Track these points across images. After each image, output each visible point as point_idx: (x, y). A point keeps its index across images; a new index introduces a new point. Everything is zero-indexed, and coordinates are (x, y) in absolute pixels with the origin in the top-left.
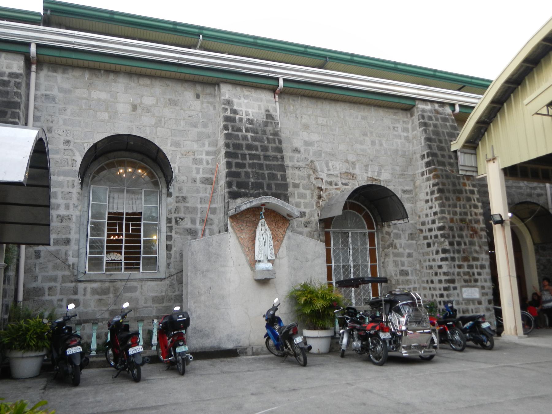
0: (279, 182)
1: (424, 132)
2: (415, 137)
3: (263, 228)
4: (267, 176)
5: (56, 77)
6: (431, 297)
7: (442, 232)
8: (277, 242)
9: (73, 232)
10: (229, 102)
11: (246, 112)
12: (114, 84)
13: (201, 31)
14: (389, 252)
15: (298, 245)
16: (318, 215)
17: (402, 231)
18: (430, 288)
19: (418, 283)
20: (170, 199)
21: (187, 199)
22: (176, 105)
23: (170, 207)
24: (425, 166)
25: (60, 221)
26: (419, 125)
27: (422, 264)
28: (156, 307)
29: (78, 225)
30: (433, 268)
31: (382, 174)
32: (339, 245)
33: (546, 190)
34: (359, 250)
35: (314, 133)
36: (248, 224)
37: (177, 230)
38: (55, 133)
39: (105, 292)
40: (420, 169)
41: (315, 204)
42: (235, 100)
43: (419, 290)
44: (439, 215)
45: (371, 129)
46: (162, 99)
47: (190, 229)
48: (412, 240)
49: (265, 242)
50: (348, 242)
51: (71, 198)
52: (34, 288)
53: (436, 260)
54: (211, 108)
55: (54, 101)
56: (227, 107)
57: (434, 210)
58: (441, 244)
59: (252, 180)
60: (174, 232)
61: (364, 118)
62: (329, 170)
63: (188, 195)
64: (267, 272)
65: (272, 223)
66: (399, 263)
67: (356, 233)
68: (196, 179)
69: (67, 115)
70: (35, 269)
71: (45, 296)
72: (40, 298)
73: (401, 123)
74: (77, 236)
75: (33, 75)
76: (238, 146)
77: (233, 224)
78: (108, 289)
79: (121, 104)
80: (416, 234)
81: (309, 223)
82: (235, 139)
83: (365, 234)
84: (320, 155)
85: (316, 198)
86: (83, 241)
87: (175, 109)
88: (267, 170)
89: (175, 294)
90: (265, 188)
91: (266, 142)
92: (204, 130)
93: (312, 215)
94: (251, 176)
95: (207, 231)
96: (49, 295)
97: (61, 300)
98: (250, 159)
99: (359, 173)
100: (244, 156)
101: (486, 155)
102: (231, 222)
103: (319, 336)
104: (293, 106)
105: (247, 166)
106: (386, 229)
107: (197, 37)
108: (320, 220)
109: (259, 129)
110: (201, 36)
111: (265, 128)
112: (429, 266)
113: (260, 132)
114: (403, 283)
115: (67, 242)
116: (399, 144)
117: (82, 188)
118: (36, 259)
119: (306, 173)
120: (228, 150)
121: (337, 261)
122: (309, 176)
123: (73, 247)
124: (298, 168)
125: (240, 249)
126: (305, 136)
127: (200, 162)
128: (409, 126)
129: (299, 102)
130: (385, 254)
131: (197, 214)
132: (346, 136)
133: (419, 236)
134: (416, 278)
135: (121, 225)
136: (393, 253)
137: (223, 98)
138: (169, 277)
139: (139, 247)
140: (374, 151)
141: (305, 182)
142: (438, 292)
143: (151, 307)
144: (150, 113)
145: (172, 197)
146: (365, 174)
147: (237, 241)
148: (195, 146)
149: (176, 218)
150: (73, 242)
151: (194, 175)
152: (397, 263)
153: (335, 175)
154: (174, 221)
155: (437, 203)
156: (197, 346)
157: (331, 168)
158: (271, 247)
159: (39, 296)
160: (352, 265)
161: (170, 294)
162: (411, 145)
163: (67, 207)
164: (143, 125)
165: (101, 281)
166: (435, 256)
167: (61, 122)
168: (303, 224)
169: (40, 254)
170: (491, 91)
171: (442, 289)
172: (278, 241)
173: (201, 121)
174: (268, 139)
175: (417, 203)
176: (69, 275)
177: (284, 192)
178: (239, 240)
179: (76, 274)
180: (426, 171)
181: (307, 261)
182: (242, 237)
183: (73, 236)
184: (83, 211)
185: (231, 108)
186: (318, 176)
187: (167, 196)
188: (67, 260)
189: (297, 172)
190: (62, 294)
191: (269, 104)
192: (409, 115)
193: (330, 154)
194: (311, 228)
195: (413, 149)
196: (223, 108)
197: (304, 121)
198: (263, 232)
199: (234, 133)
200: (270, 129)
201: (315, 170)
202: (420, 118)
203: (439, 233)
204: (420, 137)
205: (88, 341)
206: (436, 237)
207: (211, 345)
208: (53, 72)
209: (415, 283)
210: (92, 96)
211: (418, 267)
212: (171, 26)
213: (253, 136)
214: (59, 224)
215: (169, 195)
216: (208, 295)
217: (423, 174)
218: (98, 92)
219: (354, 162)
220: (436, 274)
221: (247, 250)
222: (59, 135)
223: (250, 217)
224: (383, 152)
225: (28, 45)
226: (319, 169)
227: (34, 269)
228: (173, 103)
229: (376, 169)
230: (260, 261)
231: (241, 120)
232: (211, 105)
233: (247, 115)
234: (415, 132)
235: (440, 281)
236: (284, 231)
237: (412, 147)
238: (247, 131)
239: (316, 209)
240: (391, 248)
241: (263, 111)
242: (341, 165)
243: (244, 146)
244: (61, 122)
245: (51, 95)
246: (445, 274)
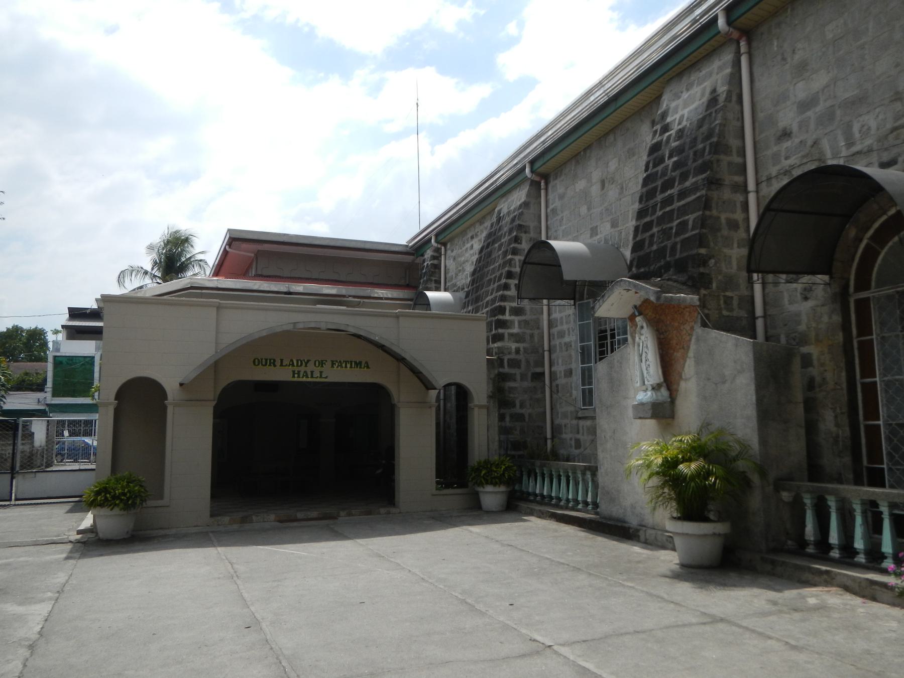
153: (865, 150)
181: (724, 382)
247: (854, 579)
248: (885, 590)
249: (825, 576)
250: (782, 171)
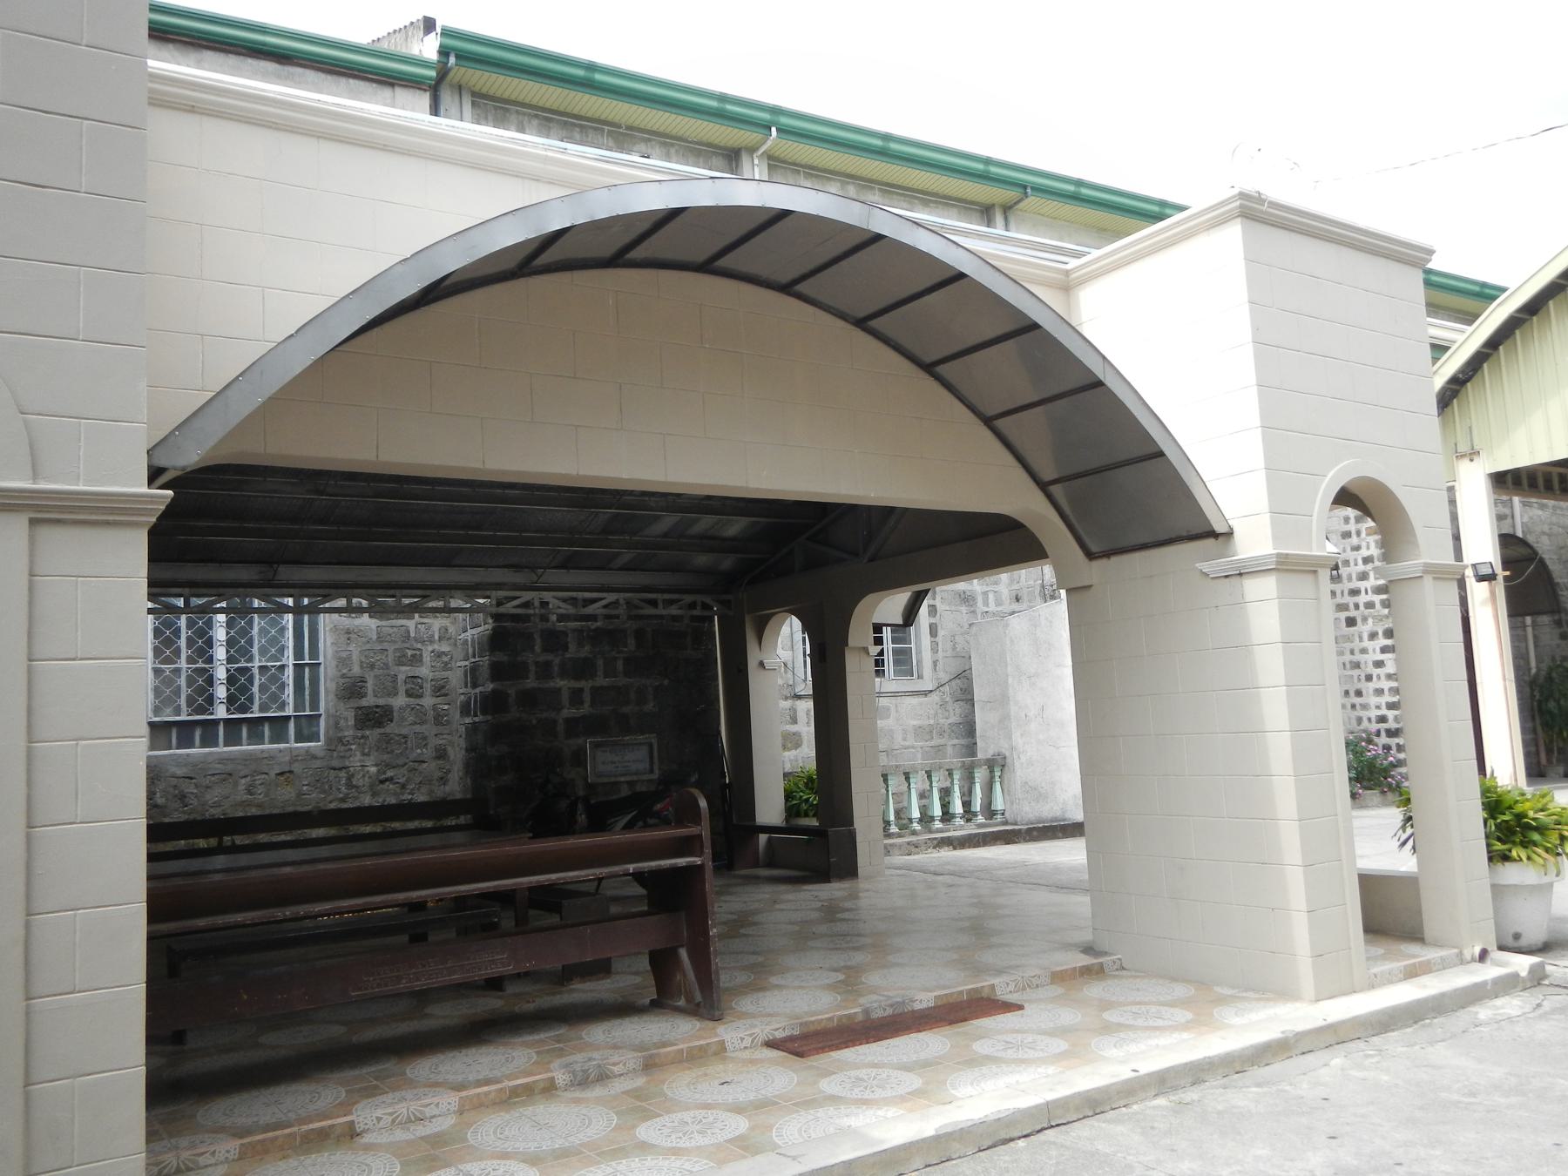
6: (1354, 722)
7: (1384, 597)
13: (775, 118)
18: (1353, 706)
30: (1362, 666)
33: (1512, 507)
44: (1377, 563)
53: (1370, 651)
57: (1364, 553)
58: (1381, 620)
89: (950, 721)
95: (991, 596)
101: (1456, 445)
107: (766, 132)
110: (774, 129)
112: (1351, 662)
138: (938, 688)
142: (1374, 713)
143: (913, 747)
155: (1373, 539)
161: (942, 721)
166: (1366, 643)
170: (1484, 324)
171: (1384, 706)
203: (1377, 599)
206: (1370, 605)
212: (714, 104)
220: (1369, 678)
235: (1379, 692)
246: (1389, 677)
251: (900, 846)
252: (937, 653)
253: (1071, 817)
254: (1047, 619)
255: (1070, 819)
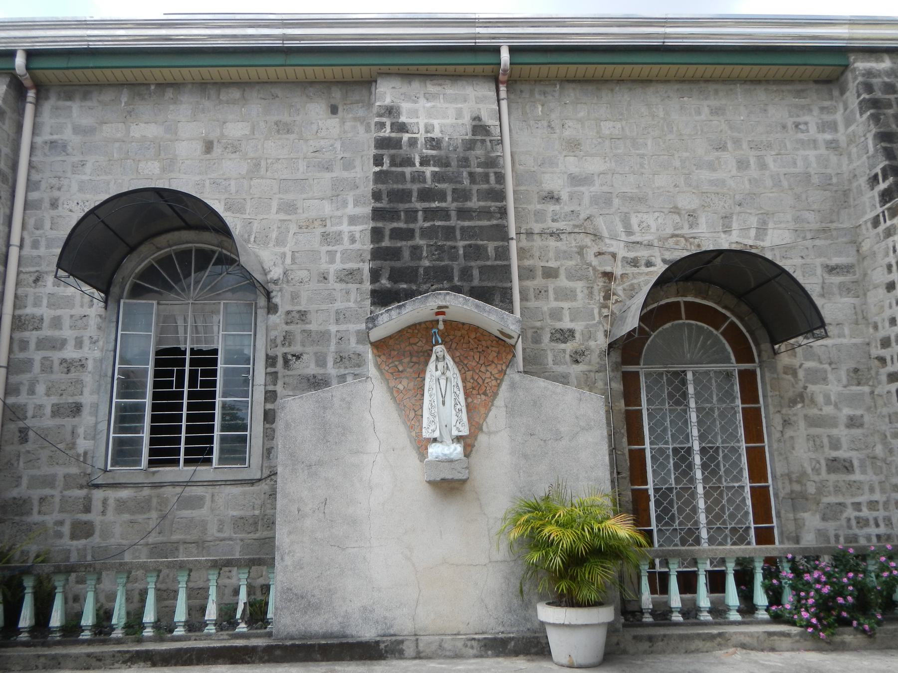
0: (489, 263)
1: (871, 122)
2: (851, 141)
3: (441, 365)
4: (461, 252)
5: (70, 107)
8: (483, 397)
9: (86, 391)
10: (391, 111)
11: (426, 126)
12: (172, 107)
14: (795, 415)
15: (535, 403)
16: (606, 336)
17: (830, 364)
19: (883, 491)
20: (274, 319)
21: (308, 316)
22: (288, 132)
23: (273, 334)
24: (880, 201)
25: (66, 370)
26: (861, 108)
27: (890, 443)
28: (242, 540)
29: (97, 378)
31: (770, 232)
32: (663, 403)
34: (716, 413)
35: (592, 155)
36: (414, 359)
37: (287, 379)
38: (63, 208)
39: (143, 506)
40: (868, 210)
41: (596, 311)
42: (405, 106)
43: (886, 508)
45: (735, 134)
46: (262, 124)
47: (314, 377)
48: (859, 384)
49: (443, 397)
50: (685, 395)
51: (85, 327)
52: (15, 498)
54: (361, 129)
55: (64, 151)
56: (384, 120)
59: (426, 263)
60: (280, 383)
61: (715, 112)
62: (629, 233)
63: (312, 307)
64: (446, 464)
65: (472, 353)
66: (826, 441)
67: (707, 373)
68: (328, 273)
69: (85, 174)
70: (18, 463)
71: (32, 514)
72: (24, 518)
73: (816, 112)
74: (94, 398)
75: (29, 109)
76: (403, 196)
77: (378, 359)
78: (148, 500)
79: (185, 143)
80: (869, 369)
81: (583, 354)
82: (397, 182)
83: (729, 375)
84: (608, 202)
85: (599, 297)
86: (103, 409)
87: (287, 139)
88: (461, 240)
90: (456, 279)
91: (466, 182)
92: (345, 174)
93: (589, 335)
94: (425, 254)
96: (39, 512)
97: (61, 523)
98: (425, 219)
99: (707, 235)
100: (411, 215)
102: (376, 356)
103: (567, 623)
104: (543, 105)
105: (417, 234)
106: (785, 359)
108: (611, 346)
109: (453, 156)
111: (468, 153)
113: (454, 163)
114: (837, 490)
115: (76, 409)
116: (812, 159)
117: (106, 308)
118: (21, 443)
119: (574, 244)
120: (379, 205)
121: (657, 438)
122: (581, 251)
123: (87, 419)
124: (556, 235)
125: (394, 415)
126: (571, 164)
127: (337, 238)
128: (839, 117)
129: (557, 94)
130: (785, 421)
131: (329, 345)
132: (673, 155)
133: (877, 373)
134: (874, 478)
135: (181, 374)
136: (806, 416)
137: (378, 104)
138: (270, 476)
139: (212, 417)
140: (747, 182)
141: (571, 263)
143: (231, 539)
144: (238, 153)
145: (278, 314)
146: (723, 236)
147: (387, 397)
148: (327, 209)
149: (285, 356)
150: (86, 411)
151: (324, 266)
152: (818, 443)
153: (645, 242)
154: (280, 361)
156: (293, 630)
157: (636, 228)
158: (458, 407)
159: (22, 514)
160: (696, 447)
162: (845, 160)
163: (79, 344)
164: (225, 177)
165: (137, 486)
167: (75, 187)
168: (567, 357)
169: (27, 434)
172: (485, 394)
173: (340, 157)
174: (471, 175)
175: (869, 294)
176: (76, 474)
177: (500, 285)
178: (392, 393)
179: (89, 471)
180: (883, 212)
181: (559, 439)
182: (401, 387)
183: (87, 398)
184: (107, 350)
185: (394, 120)
186: (604, 249)
187: (268, 313)
188: (74, 444)
189: (552, 243)
190: (62, 512)
191: (481, 106)
192: (836, 93)
193: (632, 199)
194: (589, 363)
195: (851, 167)
196: (377, 123)
197: (567, 133)
198: (439, 373)
199: (393, 169)
200: (479, 152)
201: (595, 235)
202: (861, 91)
204: (864, 136)
205: (107, 606)
207: (324, 630)
208: (66, 100)
209: (872, 490)
210: (132, 134)
211: (879, 450)
213: (436, 172)
214: (64, 376)
215: (272, 308)
216: (321, 515)
217: (876, 222)
218: (142, 125)
219: (694, 211)
221: (412, 415)
222: (71, 211)
223: (420, 344)
224: (769, 183)
225: (11, 54)
226: (605, 234)
227: (16, 464)
228: (284, 128)
229: (753, 221)
230: (435, 440)
231: (413, 142)
232: (362, 123)
233: (427, 132)
234: (853, 128)
236: (500, 372)
237: (848, 165)
238: (425, 162)
239: (600, 322)
240: (800, 406)
241: (467, 120)
242: (660, 221)
243: (415, 194)
244: (75, 187)
245: (60, 142)
247: (751, 635)
248: (783, 638)
249: (719, 639)
250: (548, 231)
251: (77, 657)
252: (273, 439)
253: (354, 633)
254: (343, 400)
255: (352, 637)
